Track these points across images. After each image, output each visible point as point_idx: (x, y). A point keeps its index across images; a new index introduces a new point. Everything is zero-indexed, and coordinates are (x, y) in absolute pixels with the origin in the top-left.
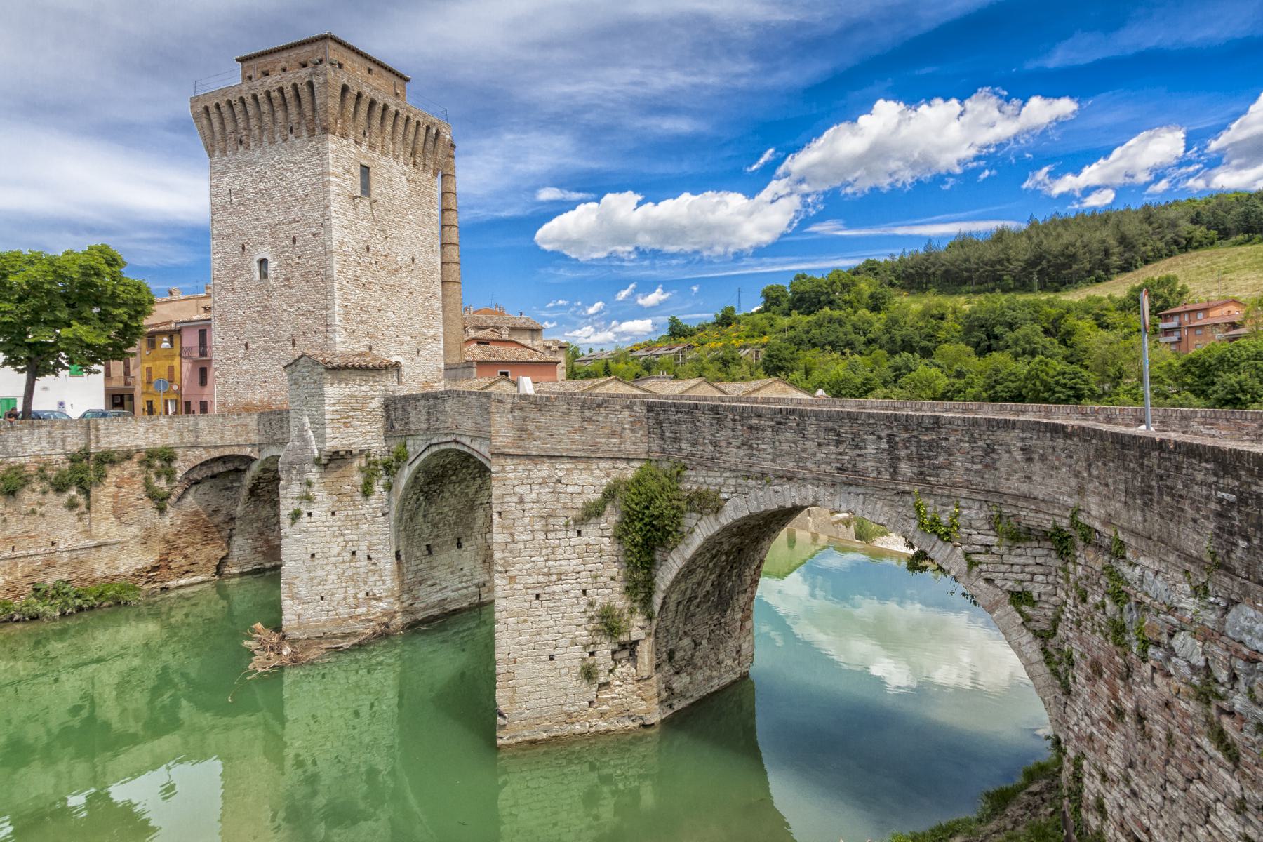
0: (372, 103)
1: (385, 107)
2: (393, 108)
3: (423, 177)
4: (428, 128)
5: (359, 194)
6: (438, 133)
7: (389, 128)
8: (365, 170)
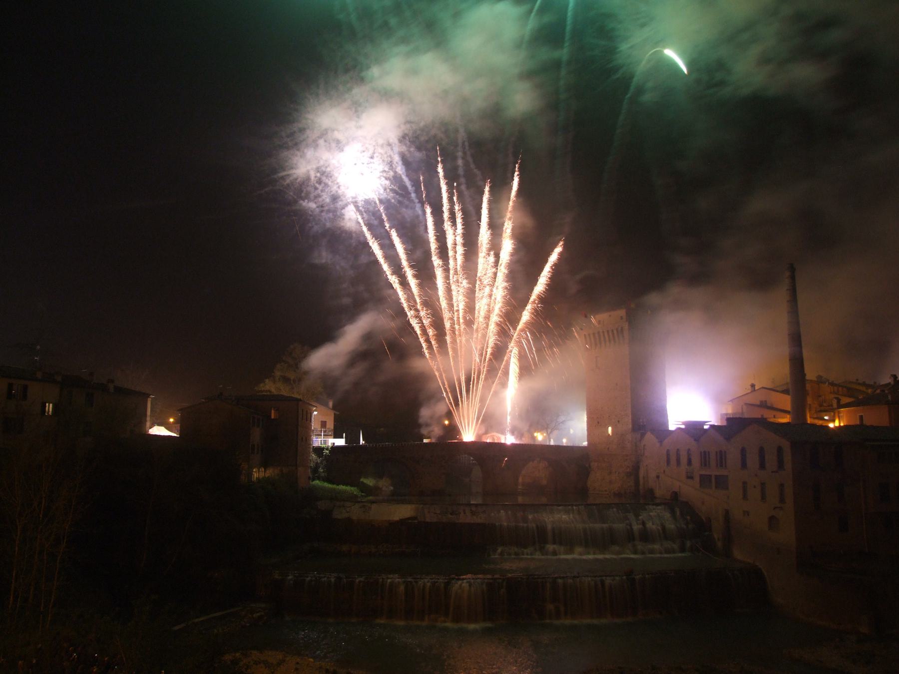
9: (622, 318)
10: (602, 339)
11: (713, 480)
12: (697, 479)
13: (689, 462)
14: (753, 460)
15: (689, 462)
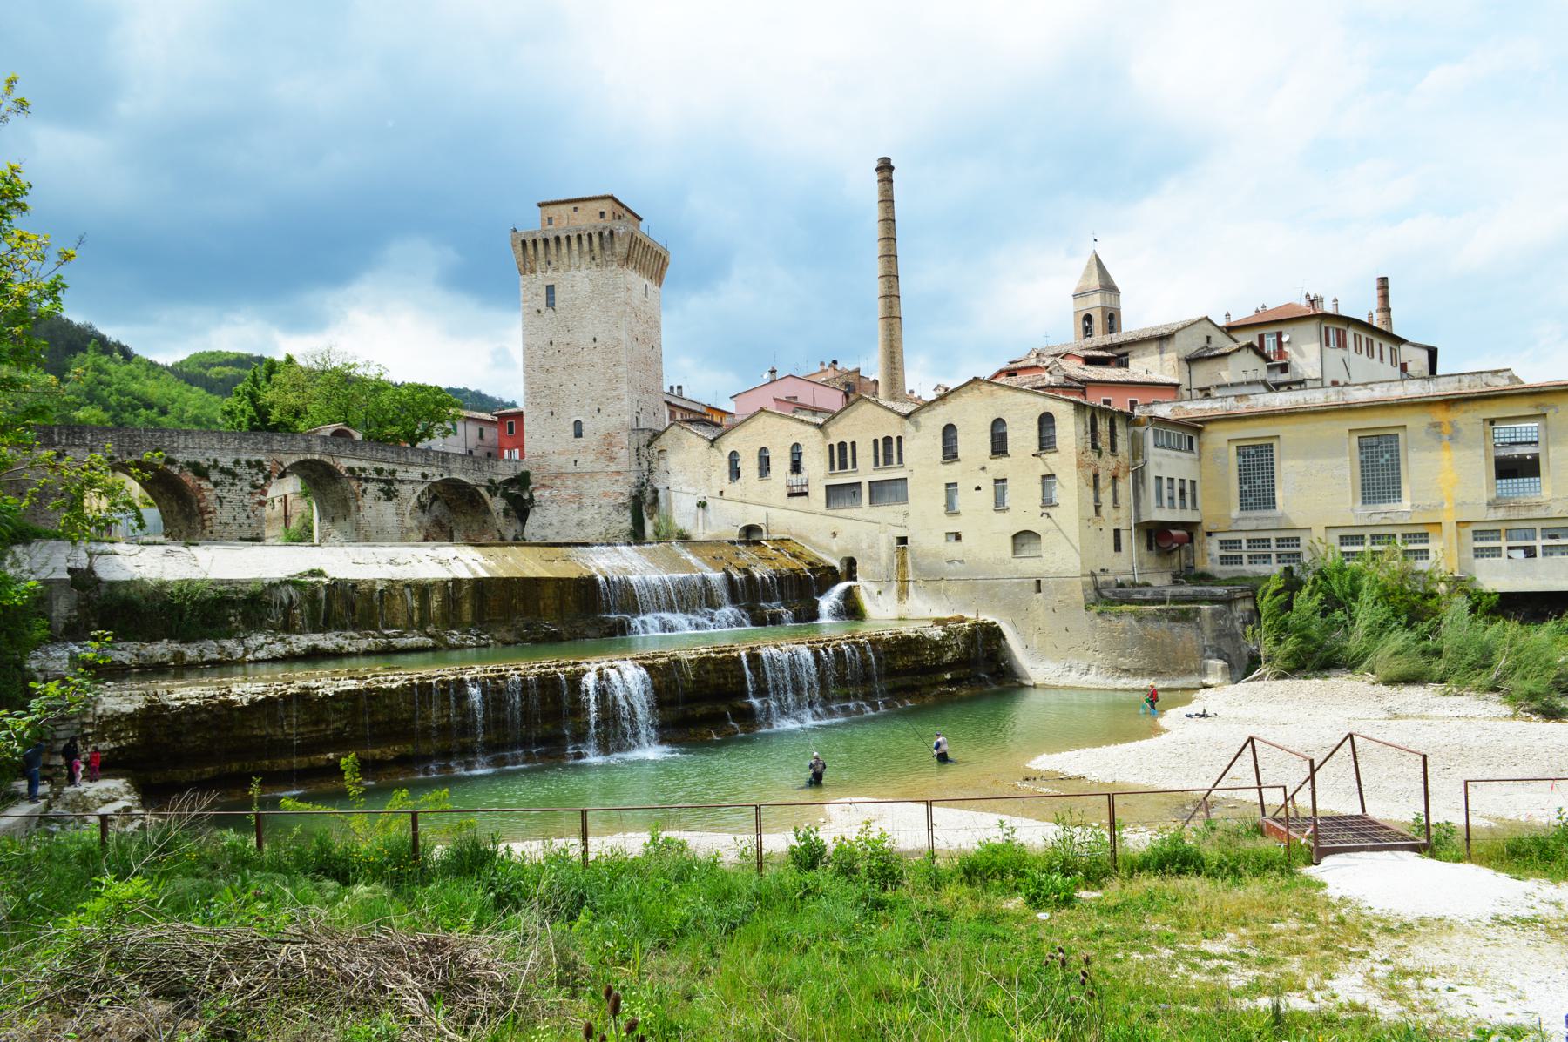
0: (546, 241)
1: (557, 239)
2: (563, 237)
3: (607, 271)
4: (601, 234)
5: (543, 307)
6: (611, 233)
7: (564, 249)
8: (550, 289)
9: (602, 214)
10: (564, 249)
11: (865, 489)
12: (818, 494)
13: (796, 468)
14: (973, 443)
15: (796, 468)
